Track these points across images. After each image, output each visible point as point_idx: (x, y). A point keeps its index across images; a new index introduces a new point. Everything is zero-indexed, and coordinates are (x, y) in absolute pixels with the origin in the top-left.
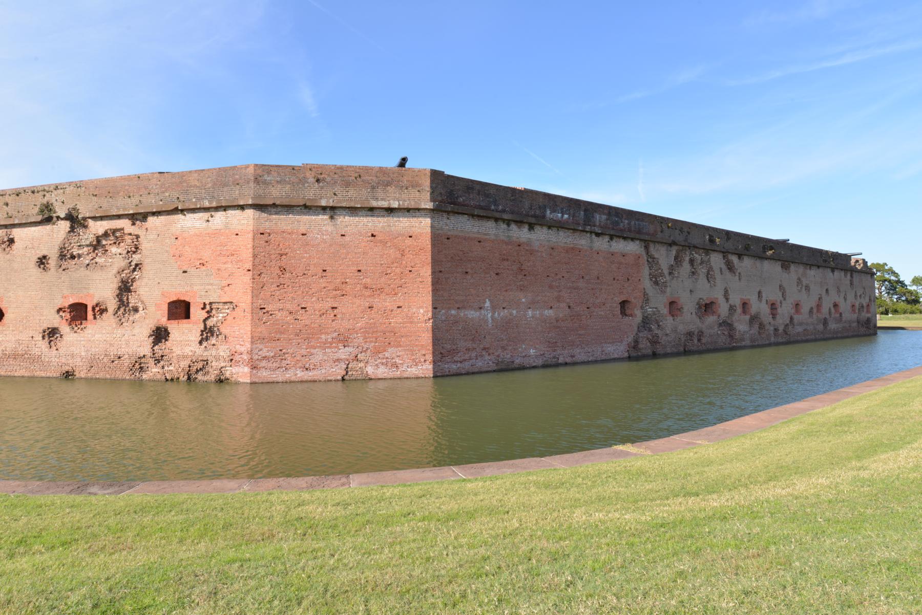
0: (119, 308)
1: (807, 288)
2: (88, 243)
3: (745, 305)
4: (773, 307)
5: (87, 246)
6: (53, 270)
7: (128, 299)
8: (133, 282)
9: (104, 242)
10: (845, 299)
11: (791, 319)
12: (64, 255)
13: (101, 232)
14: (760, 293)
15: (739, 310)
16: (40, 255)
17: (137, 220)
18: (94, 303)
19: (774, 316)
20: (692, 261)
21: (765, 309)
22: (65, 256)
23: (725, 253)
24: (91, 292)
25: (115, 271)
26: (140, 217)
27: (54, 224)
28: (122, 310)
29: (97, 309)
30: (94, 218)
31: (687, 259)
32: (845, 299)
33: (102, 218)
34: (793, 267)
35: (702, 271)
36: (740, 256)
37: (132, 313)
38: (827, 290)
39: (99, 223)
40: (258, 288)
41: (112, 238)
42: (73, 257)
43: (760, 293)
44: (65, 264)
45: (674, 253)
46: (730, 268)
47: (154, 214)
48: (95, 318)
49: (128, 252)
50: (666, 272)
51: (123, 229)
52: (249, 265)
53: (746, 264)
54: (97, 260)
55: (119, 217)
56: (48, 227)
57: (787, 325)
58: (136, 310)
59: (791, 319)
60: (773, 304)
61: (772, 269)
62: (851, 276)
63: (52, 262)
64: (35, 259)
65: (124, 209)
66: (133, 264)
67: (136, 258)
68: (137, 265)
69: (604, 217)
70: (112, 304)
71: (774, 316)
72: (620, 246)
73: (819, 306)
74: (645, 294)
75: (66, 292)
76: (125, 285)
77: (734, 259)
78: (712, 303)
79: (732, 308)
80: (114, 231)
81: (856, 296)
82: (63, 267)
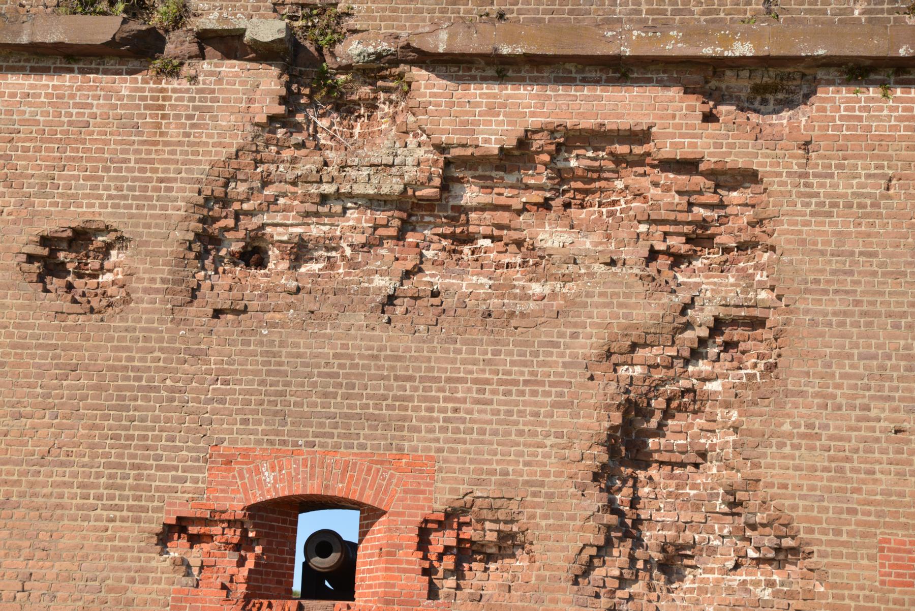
0: (604, 550)
2: (392, 186)
5: (375, 202)
6: (149, 309)
7: (634, 502)
8: (667, 414)
9: (471, 194)
12: (221, 238)
13: (493, 137)
16: (59, 219)
17: (721, 100)
18: (439, 501)
22: (217, 242)
24: (416, 443)
25: (588, 345)
26: (742, 84)
27: (173, 72)
28: (620, 554)
29: (442, 540)
30: (456, 65)
33: (501, 68)
37: (660, 580)
39: (480, 93)
41: (542, 177)
42: (253, 255)
44: (224, 282)
47: (859, 71)
48: (433, 593)
49: (653, 255)
51: (643, 136)
54: (431, 278)
55: (619, 70)
56: (128, 87)
58: (672, 563)
63: (140, 268)
64: (25, 239)
65: (691, 33)
66: (703, 315)
67: (712, 288)
68: (718, 326)
70: (565, 522)
75: (232, 435)
76: (627, 424)
80: (571, 139)
82: (210, 298)
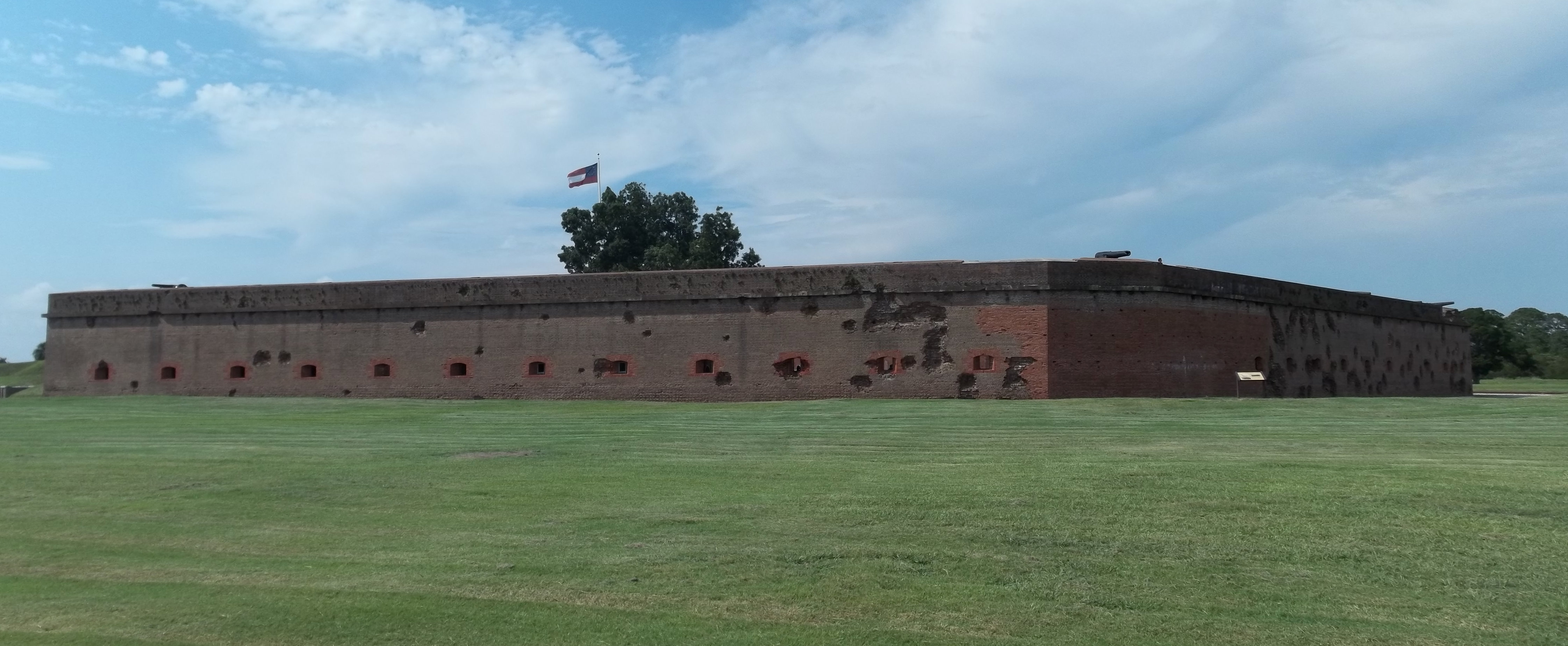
1: (1398, 344)
3: (1343, 361)
4: (1367, 364)
10: (1437, 357)
11: (1384, 376)
14: (1355, 350)
15: (1339, 367)
19: (1368, 372)
20: (1302, 320)
21: (1360, 367)
23: (1327, 312)
25: (922, 334)
31: (1298, 318)
32: (1437, 357)
34: (1384, 323)
35: (1310, 329)
36: (1338, 313)
38: (1417, 346)
40: (1051, 348)
43: (1355, 350)
45: (1289, 313)
46: (1331, 325)
50: (1284, 331)
52: (1045, 332)
53: (1342, 322)
57: (1380, 383)
59: (1384, 376)
60: (1367, 361)
61: (1365, 325)
62: (1443, 330)
69: (1244, 286)
71: (1368, 372)
72: (1255, 310)
73: (1409, 364)
74: (1271, 351)
77: (1334, 316)
78: (1318, 360)
79: (1333, 366)
81: (1448, 352)
